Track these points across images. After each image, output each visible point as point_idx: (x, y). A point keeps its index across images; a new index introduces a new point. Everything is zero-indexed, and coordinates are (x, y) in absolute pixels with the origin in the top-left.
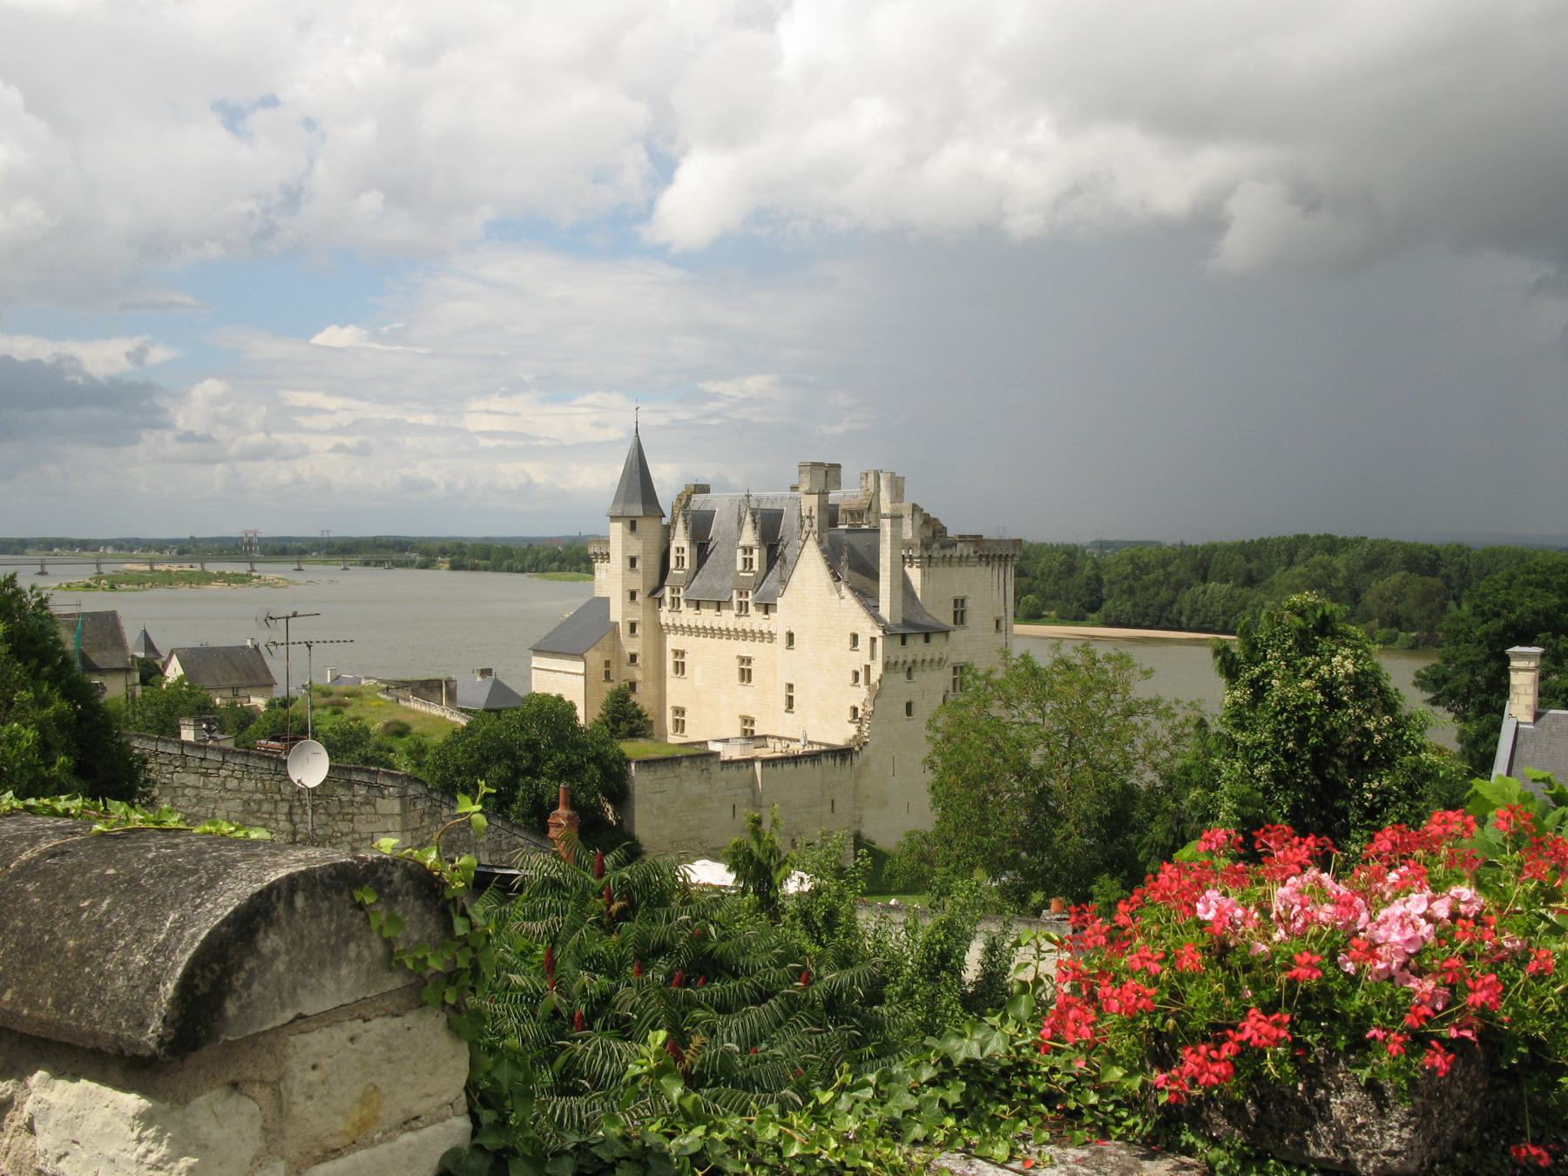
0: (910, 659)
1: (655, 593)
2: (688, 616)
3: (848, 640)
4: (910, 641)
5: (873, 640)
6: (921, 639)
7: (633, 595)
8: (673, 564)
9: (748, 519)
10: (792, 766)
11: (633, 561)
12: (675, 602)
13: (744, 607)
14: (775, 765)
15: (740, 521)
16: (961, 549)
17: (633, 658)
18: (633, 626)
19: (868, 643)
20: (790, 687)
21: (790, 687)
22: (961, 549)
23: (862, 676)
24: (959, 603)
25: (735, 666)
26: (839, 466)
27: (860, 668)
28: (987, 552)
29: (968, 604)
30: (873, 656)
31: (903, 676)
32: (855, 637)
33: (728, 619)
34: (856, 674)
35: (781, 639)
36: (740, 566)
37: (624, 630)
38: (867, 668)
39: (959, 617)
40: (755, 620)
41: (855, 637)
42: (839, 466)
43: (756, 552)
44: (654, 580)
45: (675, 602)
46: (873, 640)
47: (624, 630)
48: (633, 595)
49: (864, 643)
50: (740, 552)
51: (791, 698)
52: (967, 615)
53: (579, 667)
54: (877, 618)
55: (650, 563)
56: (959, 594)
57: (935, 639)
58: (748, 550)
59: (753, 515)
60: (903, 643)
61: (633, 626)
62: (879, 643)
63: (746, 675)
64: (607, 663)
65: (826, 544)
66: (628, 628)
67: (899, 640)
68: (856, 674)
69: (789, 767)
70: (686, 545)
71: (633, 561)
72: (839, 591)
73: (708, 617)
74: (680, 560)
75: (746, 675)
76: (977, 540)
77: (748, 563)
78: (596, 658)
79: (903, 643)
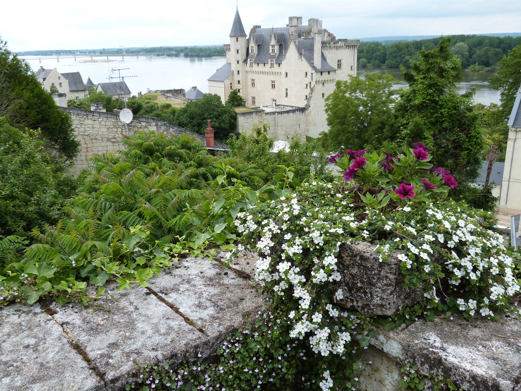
0: (323, 80)
1: (245, 61)
2: (255, 68)
3: (304, 74)
4: (323, 74)
5: (312, 74)
6: (327, 73)
7: (238, 62)
8: (250, 51)
9: (273, 36)
10: (287, 114)
13: (272, 66)
14: (281, 114)
15: (271, 36)
16: (340, 44)
17: (239, 82)
18: (238, 72)
19: (310, 75)
20: (287, 89)
21: (287, 89)
22: (340, 44)
24: (339, 61)
25: (270, 83)
26: (301, 18)
27: (308, 83)
28: (348, 44)
29: (342, 62)
30: (312, 79)
31: (321, 85)
32: (306, 73)
33: (268, 67)
35: (284, 75)
39: (339, 66)
40: (276, 68)
41: (306, 73)
42: (301, 18)
43: (275, 47)
44: (244, 57)
46: (312, 74)
48: (238, 62)
49: (309, 75)
50: (271, 47)
51: (287, 93)
52: (342, 65)
53: (222, 85)
54: (314, 68)
55: (243, 51)
56: (339, 59)
57: (331, 73)
58: (273, 46)
59: (275, 35)
60: (321, 74)
61: (238, 72)
62: (314, 75)
63: (273, 86)
64: (231, 84)
65: (297, 43)
66: (237, 72)
67: (320, 73)
69: (286, 115)
70: (254, 45)
72: (301, 58)
74: (252, 52)
75: (273, 86)
76: (345, 40)
77: (273, 51)
78: (227, 82)
79: (321, 74)
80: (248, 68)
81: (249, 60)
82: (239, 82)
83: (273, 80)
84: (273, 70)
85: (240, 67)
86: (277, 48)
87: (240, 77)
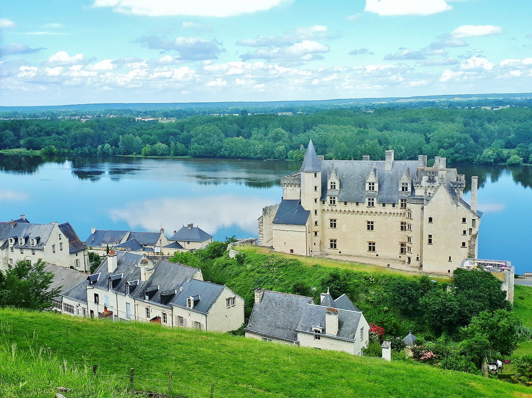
5: (474, 220)
8: (329, 187)
11: (316, 188)
12: (333, 202)
17: (316, 223)
18: (316, 212)
21: (430, 236)
23: (467, 232)
32: (464, 220)
33: (364, 207)
34: (465, 232)
36: (367, 189)
37: (313, 213)
38: (471, 229)
41: (464, 220)
45: (333, 202)
46: (474, 220)
47: (313, 213)
50: (367, 185)
61: (316, 212)
62: (477, 221)
68: (465, 232)
71: (316, 188)
73: (351, 207)
74: (333, 187)
80: (327, 206)
81: (328, 199)
82: (316, 223)
83: (370, 220)
84: (372, 209)
85: (318, 206)
86: (376, 186)
87: (317, 218)
